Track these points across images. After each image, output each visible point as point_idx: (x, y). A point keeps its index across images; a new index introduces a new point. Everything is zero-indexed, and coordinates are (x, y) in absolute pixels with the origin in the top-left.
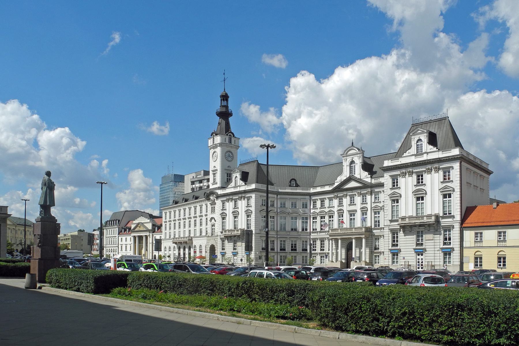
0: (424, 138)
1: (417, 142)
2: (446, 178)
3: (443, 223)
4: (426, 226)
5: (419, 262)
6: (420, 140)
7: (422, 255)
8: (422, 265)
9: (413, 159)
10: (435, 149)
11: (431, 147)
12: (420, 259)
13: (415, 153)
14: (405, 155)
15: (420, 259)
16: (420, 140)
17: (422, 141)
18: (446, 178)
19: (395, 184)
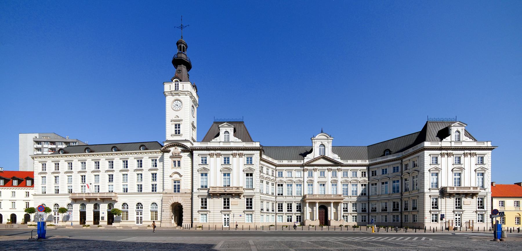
0: (231, 130)
1: (225, 133)
2: (250, 161)
3: (245, 193)
4: (233, 194)
5: (225, 221)
6: (227, 132)
7: (228, 215)
8: (228, 223)
9: (222, 145)
10: (240, 140)
11: (236, 138)
12: (226, 219)
13: (224, 141)
14: (213, 140)
15: (226, 219)
16: (227, 132)
17: (229, 133)
18: (250, 161)
19: (204, 162)
